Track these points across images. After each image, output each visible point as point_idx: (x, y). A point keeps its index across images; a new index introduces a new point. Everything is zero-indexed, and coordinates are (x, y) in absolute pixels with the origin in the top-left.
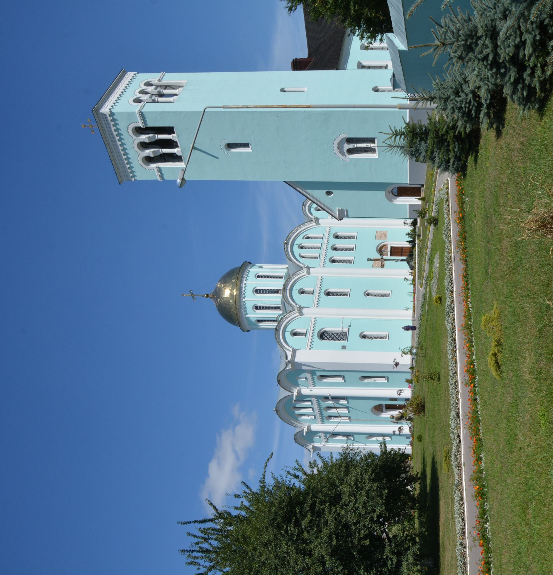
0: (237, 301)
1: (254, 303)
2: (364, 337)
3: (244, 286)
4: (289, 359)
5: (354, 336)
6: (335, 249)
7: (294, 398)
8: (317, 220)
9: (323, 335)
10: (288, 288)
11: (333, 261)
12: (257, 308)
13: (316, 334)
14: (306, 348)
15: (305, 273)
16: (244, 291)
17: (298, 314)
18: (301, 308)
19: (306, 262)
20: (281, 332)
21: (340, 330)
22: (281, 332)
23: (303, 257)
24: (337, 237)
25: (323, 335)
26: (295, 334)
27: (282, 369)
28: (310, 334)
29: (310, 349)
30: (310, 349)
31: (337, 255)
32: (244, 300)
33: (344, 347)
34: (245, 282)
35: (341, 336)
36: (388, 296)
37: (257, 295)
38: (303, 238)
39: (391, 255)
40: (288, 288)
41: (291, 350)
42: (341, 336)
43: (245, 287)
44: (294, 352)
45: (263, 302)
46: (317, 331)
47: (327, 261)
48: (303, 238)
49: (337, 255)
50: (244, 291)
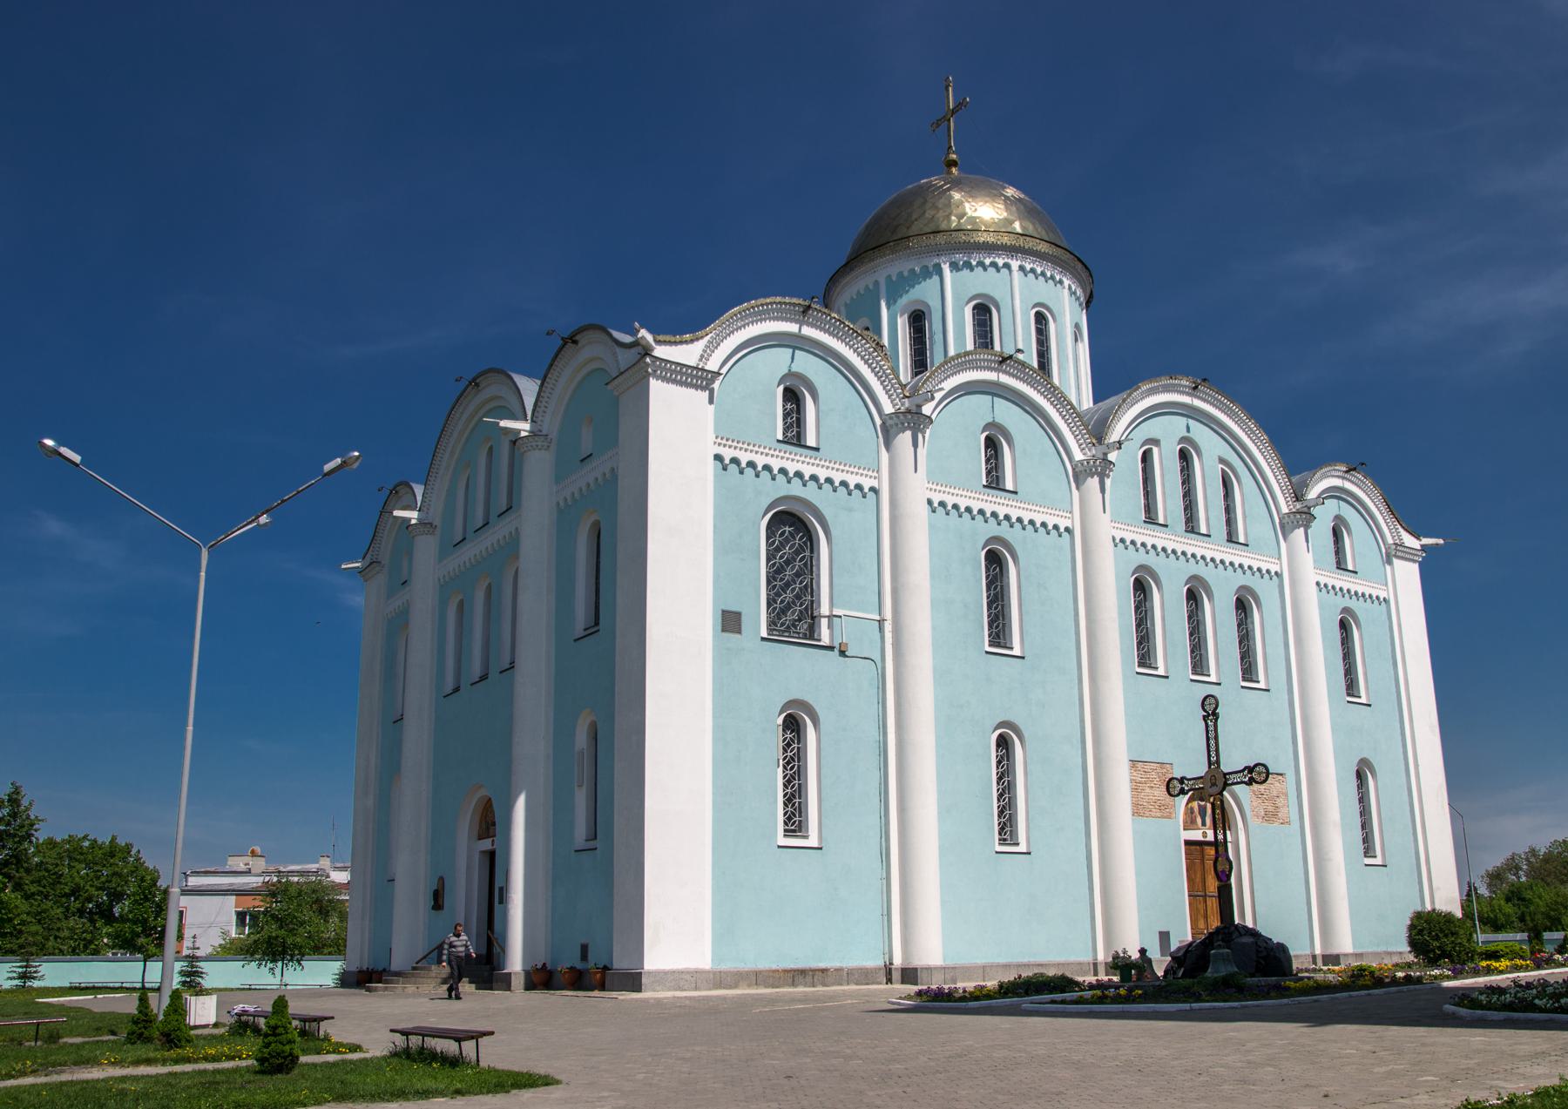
0: (940, 239)
1: (934, 304)
2: (793, 725)
3: (1000, 262)
4: (661, 351)
5: (797, 671)
6: (1192, 596)
7: (503, 423)
8: (1304, 517)
9: (793, 530)
10: (1005, 379)
11: (1140, 587)
12: (918, 320)
13: (796, 489)
14: (722, 438)
15: (1078, 456)
16: (981, 264)
17: (888, 409)
18: (913, 420)
19: (1125, 461)
20: (792, 328)
21: (825, 609)
22: (792, 328)
23: (1146, 458)
24: (1242, 606)
25: (793, 530)
26: (792, 397)
27: (616, 334)
28: (794, 462)
29: (718, 458)
30: (718, 458)
31: (1168, 608)
32: (946, 268)
33: (730, 622)
34: (1015, 264)
35: (794, 610)
36: (1003, 841)
37: (968, 312)
38: (1222, 461)
39: (1187, 843)
40: (1005, 379)
41: (712, 365)
42: (794, 610)
43: (994, 264)
44: (699, 379)
45: (938, 337)
46: (810, 493)
47: (1142, 558)
48: (1222, 461)
49: (1168, 608)
50: (981, 264)
